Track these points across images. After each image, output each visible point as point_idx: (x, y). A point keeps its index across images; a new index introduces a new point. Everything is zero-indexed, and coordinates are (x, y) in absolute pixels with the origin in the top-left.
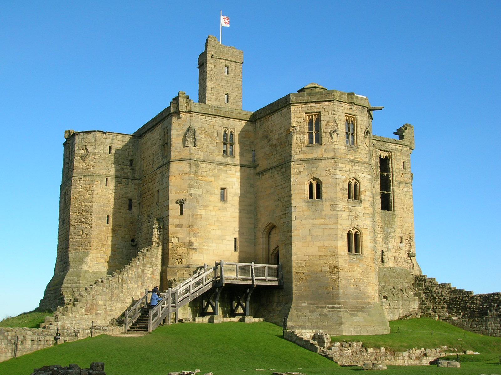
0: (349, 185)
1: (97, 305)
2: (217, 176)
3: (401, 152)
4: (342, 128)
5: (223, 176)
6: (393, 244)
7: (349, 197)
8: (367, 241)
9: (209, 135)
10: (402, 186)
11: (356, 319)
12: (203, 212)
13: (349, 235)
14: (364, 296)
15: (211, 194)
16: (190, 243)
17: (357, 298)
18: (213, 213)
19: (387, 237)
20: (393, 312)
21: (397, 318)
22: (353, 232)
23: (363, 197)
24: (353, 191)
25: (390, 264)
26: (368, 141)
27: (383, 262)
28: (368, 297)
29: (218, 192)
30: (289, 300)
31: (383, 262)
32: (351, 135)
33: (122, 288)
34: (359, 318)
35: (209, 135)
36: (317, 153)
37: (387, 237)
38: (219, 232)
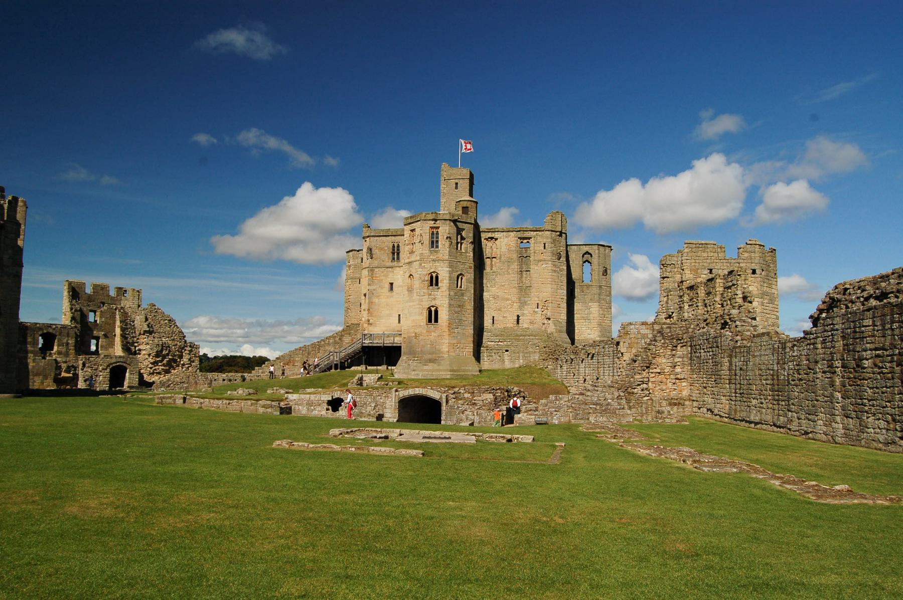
0: (432, 277)
1: (294, 361)
2: (387, 276)
3: (542, 236)
4: (427, 239)
5: (391, 275)
6: (527, 310)
7: (431, 285)
8: (443, 315)
9: (381, 249)
10: (540, 263)
11: (425, 368)
12: (376, 300)
13: (430, 312)
14: (440, 351)
15: (382, 288)
16: (369, 321)
17: (432, 353)
18: (384, 300)
19: (523, 304)
20: (513, 362)
21: (517, 366)
22: (433, 309)
23: (440, 284)
24: (434, 281)
25: (524, 324)
26: (447, 244)
27: (518, 323)
28: (442, 353)
29: (387, 286)
30: (400, 356)
31: (518, 323)
32: (434, 243)
33: (319, 349)
34: (430, 366)
35: (381, 249)
36: (414, 258)
37: (523, 304)
38: (387, 312)
